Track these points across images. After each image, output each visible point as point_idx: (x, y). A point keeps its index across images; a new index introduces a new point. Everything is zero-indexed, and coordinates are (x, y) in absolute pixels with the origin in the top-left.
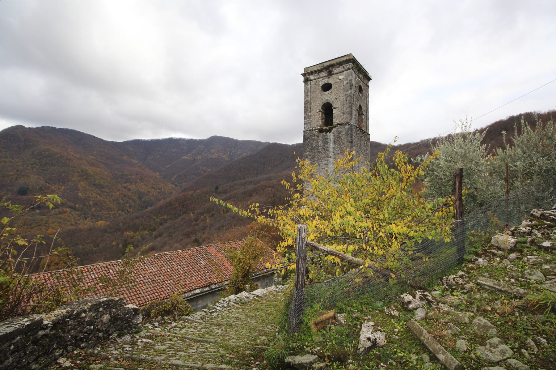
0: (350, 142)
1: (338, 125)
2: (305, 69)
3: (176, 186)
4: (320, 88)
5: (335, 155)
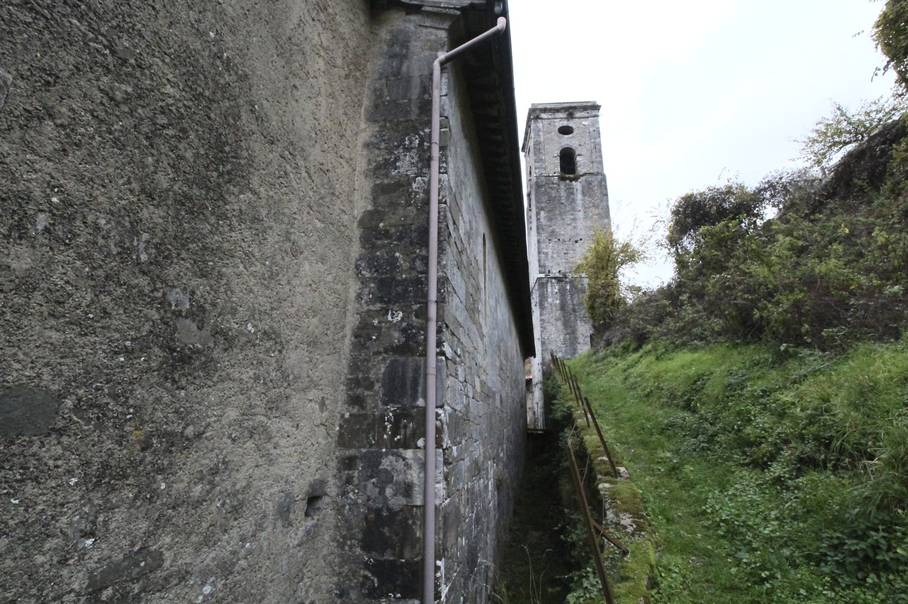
1: (585, 174)
4: (557, 129)
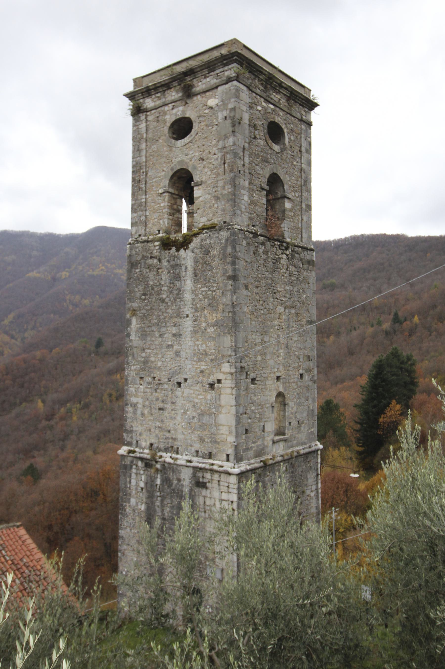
0: (229, 278)
2: (135, 80)
3: (12, 337)
5: (196, 310)
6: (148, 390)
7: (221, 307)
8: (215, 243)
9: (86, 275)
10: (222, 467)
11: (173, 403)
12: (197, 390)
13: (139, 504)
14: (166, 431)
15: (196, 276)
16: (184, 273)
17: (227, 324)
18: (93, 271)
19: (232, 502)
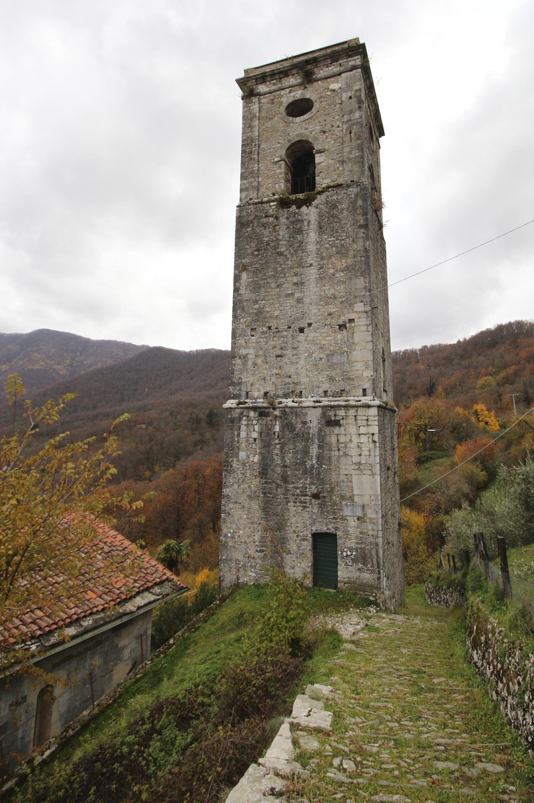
0: (361, 227)
2: (246, 71)
4: (283, 109)
5: (322, 258)
6: (262, 340)
7: (351, 253)
8: (342, 198)
9: (26, 369)
10: (360, 401)
11: (295, 348)
12: (324, 332)
13: (251, 456)
14: (286, 377)
15: (321, 228)
16: (306, 227)
17: (360, 268)
18: (33, 365)
19: (373, 434)
